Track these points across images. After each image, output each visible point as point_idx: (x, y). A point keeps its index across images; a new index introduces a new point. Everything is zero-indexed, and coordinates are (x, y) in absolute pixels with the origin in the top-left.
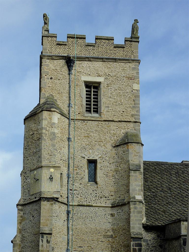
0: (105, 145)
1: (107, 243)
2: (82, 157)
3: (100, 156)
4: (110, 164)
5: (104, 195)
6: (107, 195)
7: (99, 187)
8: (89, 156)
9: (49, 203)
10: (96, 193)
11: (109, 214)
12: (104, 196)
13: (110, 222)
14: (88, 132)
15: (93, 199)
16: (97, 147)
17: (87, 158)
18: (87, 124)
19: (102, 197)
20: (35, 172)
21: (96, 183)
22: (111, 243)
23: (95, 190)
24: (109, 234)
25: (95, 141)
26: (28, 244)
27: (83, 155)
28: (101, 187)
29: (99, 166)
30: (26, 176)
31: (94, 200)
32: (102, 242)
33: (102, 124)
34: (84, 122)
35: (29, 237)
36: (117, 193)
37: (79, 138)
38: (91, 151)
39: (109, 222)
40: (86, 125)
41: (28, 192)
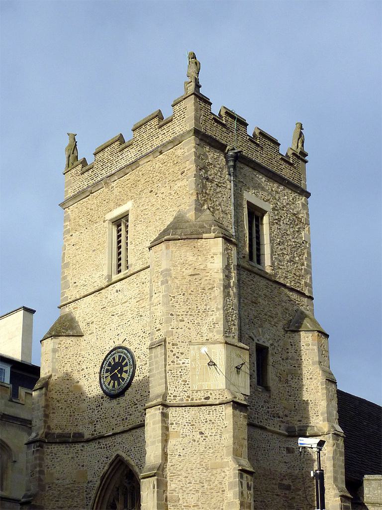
0: (277, 325)
1: (284, 499)
2: (250, 337)
3: (271, 342)
4: (283, 359)
5: (278, 412)
6: (281, 414)
7: (272, 396)
8: (258, 338)
9: (242, 413)
10: (268, 408)
11: (284, 448)
12: (278, 414)
13: (287, 461)
14: (255, 295)
15: (266, 418)
16: (267, 325)
17: (256, 341)
18: (254, 280)
19: (275, 415)
20: (204, 349)
21: (267, 389)
22: (287, 500)
23: (267, 401)
24: (285, 482)
25: (266, 315)
26: (191, 485)
27: (252, 334)
28: (273, 397)
29: (271, 359)
30: (175, 350)
31: (266, 419)
32: (277, 495)
33: (271, 286)
34: (251, 275)
35: (194, 472)
36: (296, 413)
37: (246, 301)
38: (260, 330)
39: (285, 462)
40: (253, 281)
41: (183, 383)
